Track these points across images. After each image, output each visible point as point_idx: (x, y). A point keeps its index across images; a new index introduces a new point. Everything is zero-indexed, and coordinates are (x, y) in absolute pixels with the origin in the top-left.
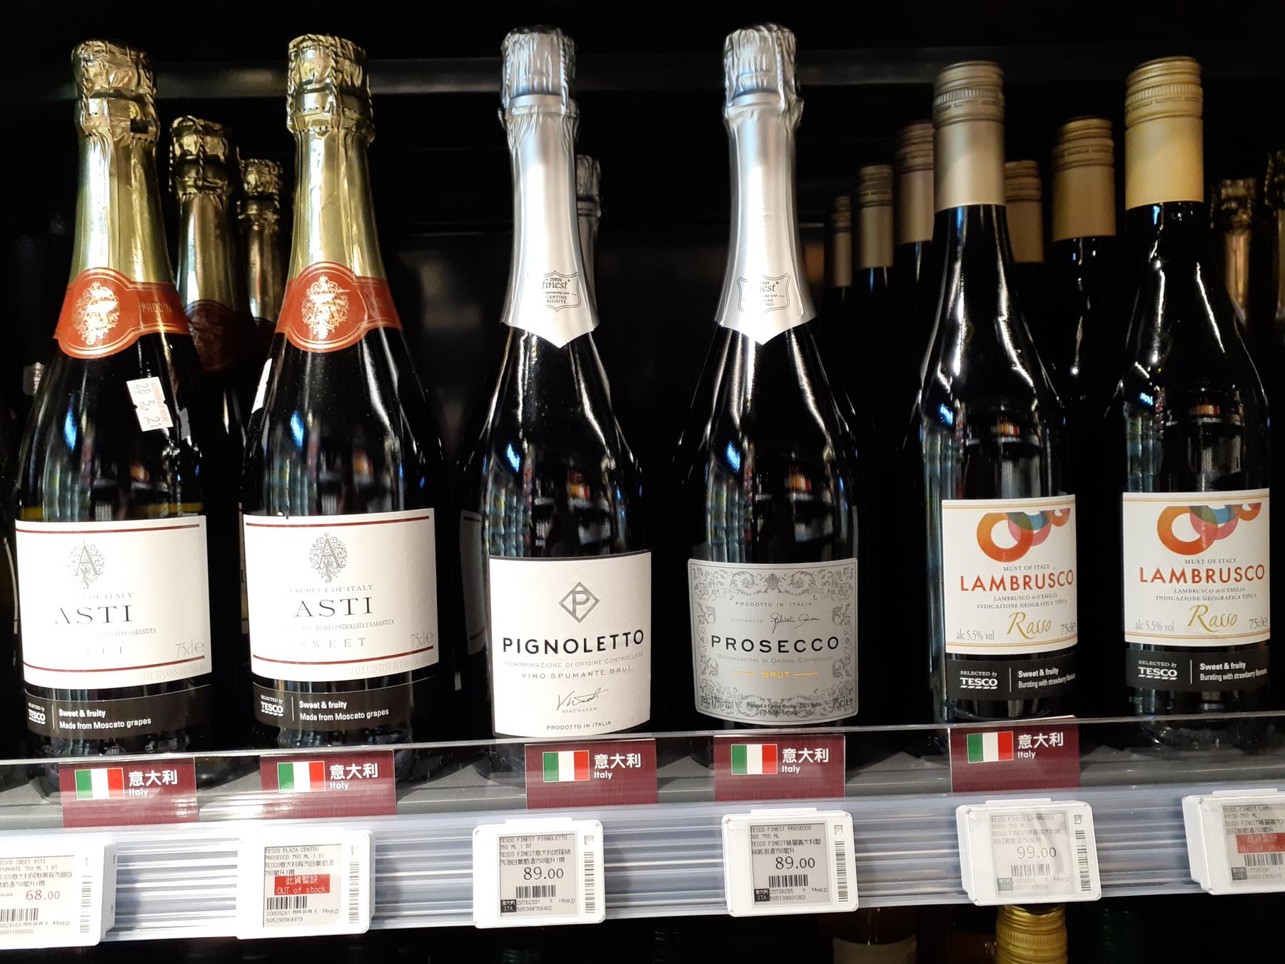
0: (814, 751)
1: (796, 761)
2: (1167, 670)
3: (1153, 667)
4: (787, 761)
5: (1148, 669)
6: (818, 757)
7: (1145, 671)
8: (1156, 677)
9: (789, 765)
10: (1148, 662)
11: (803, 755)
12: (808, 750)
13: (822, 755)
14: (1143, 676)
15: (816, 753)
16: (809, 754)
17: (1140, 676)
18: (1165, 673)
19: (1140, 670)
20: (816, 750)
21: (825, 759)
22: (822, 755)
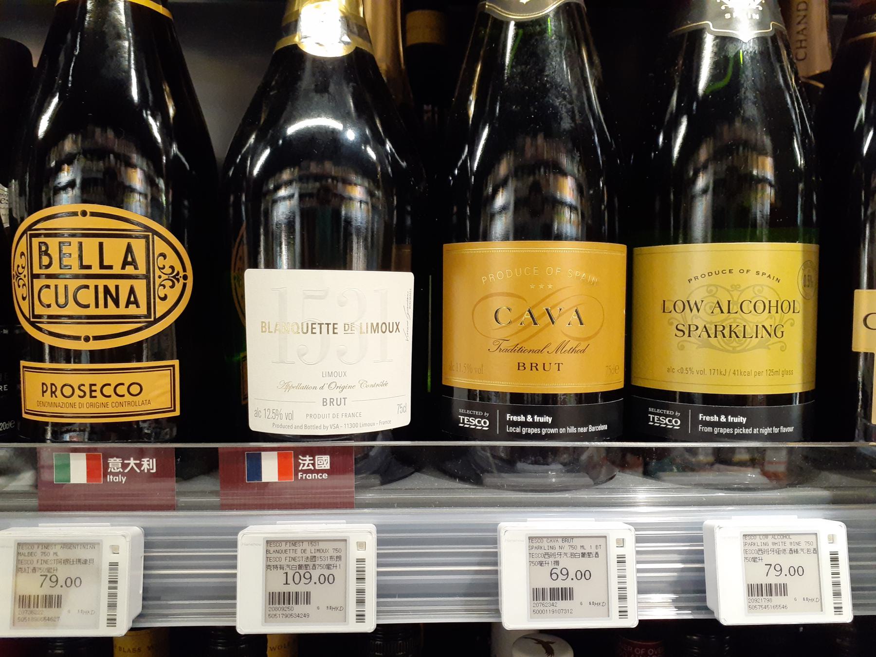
0: (141, 461)
1: (122, 471)
2: (671, 419)
3: (660, 415)
4: (113, 470)
5: (656, 417)
6: (145, 467)
7: (653, 418)
8: (662, 425)
9: (116, 474)
10: (656, 410)
11: (129, 464)
12: (134, 460)
13: (149, 465)
14: (652, 423)
15: (142, 463)
16: (135, 464)
17: (650, 423)
18: (670, 421)
19: (650, 416)
20: (143, 460)
21: (153, 469)
22: (149, 465)
